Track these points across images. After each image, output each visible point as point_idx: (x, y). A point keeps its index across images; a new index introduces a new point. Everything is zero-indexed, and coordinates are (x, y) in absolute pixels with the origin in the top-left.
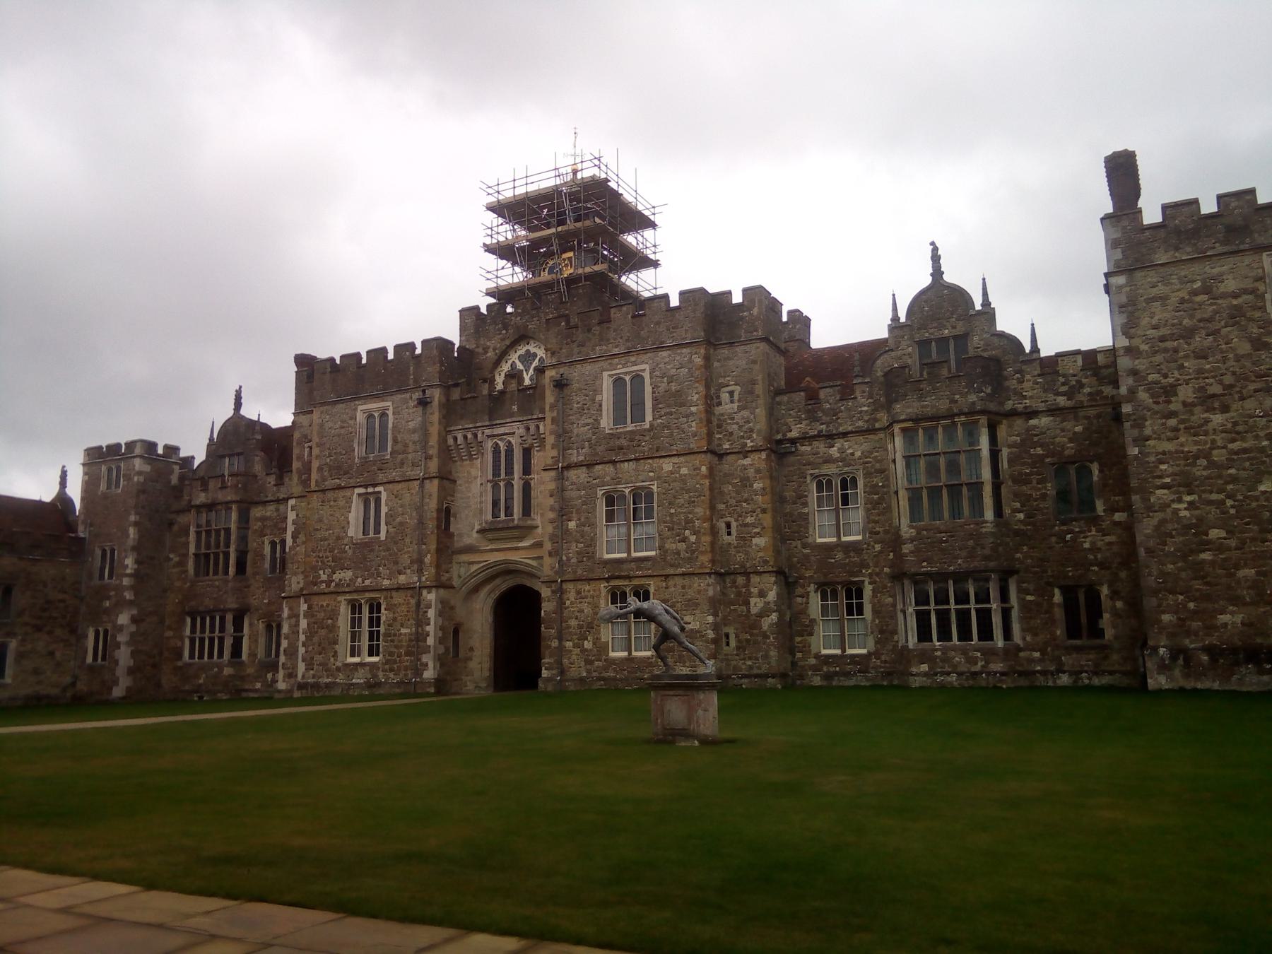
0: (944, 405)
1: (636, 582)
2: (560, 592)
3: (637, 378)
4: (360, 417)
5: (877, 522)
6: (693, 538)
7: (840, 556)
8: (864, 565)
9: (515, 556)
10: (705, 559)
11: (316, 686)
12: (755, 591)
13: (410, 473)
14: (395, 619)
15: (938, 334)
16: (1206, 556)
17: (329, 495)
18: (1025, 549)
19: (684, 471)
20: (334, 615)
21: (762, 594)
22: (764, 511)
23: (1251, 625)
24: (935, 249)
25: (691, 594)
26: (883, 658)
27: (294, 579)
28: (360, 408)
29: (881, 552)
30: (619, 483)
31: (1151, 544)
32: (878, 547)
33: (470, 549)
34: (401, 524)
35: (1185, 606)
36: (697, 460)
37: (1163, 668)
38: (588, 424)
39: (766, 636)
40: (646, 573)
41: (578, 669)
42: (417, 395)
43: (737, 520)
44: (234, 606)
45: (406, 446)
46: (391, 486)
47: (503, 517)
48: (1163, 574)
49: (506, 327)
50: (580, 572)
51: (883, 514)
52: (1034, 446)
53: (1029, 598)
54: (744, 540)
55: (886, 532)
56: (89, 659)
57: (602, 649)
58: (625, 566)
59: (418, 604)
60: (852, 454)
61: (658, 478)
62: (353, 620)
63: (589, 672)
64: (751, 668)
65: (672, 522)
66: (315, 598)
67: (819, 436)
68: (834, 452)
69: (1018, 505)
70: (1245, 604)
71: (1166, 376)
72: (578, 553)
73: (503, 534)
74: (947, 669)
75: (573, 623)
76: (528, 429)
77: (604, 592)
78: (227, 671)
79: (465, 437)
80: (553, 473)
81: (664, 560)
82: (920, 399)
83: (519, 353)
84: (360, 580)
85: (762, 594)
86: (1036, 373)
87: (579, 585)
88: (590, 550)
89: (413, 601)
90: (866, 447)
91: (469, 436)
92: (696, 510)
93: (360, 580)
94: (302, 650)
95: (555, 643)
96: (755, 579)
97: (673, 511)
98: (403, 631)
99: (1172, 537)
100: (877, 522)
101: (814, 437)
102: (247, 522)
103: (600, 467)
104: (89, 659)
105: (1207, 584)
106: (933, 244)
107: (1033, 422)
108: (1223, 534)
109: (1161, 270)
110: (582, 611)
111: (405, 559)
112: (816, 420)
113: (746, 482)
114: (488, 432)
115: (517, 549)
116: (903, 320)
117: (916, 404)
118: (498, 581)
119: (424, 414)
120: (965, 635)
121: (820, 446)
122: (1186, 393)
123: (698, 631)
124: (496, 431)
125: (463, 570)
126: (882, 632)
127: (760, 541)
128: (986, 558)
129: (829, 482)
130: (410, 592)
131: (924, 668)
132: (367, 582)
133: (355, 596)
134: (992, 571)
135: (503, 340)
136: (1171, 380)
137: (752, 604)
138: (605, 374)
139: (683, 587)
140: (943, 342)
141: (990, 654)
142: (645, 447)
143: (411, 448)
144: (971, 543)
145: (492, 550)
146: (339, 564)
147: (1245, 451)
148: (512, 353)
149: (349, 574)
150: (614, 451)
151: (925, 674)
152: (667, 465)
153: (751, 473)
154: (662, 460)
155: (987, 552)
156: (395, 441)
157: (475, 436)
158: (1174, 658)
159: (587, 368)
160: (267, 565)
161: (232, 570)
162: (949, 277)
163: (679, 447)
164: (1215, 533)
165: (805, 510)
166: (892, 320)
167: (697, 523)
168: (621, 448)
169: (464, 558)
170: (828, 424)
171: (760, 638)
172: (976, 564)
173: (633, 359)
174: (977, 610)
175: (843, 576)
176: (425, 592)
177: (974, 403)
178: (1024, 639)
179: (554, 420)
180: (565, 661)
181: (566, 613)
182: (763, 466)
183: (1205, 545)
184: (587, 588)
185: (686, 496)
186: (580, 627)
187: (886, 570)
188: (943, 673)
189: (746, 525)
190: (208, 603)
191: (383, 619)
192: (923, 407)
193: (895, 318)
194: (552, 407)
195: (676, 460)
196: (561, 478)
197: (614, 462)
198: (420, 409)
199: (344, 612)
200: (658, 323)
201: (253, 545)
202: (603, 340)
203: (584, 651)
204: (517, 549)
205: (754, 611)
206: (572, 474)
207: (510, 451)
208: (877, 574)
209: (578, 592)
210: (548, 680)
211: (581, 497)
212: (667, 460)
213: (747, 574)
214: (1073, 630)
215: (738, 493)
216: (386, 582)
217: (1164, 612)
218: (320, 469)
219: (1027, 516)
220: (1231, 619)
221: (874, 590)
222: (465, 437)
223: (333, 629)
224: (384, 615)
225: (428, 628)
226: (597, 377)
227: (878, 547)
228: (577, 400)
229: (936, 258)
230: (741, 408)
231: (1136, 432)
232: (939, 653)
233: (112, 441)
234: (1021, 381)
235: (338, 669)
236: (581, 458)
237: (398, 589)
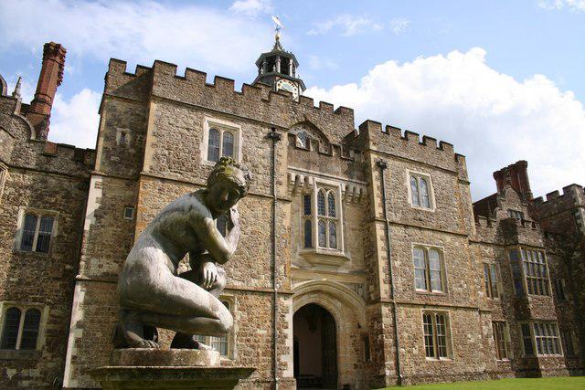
2: (393, 311)
4: (207, 128)
14: (250, 320)
19: (457, 244)
27: (94, 261)
28: (207, 119)
42: (267, 130)
49: (295, 110)
59: (274, 308)
73: (329, 261)
75: (405, 335)
79: (297, 178)
91: (302, 177)
98: (260, 332)
114: (317, 179)
118: (304, 298)
124: (324, 181)
142: (434, 225)
143: (261, 170)
157: (306, 179)
168: (420, 220)
184: (412, 310)
197: (420, 228)
198: (271, 141)
204: (336, 274)
207: (332, 198)
209: (406, 313)
210: (391, 378)
218: (156, 157)
225: (286, 331)
237: (253, 292)
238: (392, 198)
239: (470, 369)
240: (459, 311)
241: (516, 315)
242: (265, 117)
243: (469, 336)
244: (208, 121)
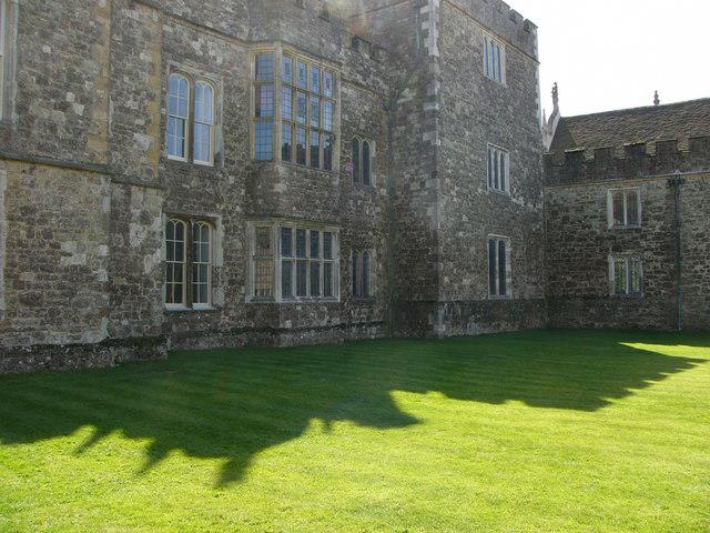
6: (79, 109)
7: (195, 183)
12: (137, 213)
16: (461, 234)
21: (145, 219)
32: (232, 180)
55: (240, 163)
64: (128, 329)
68: (196, 45)
85: (145, 219)
92: (87, 62)
96: (137, 194)
97: (47, 49)
101: (179, 18)
113: (129, 43)
123: (84, 270)
137: (132, 234)
153: (138, 35)
167: (87, 86)
187: (238, 209)
189: (128, 111)
205: (135, 243)
221: (227, 231)
227: (232, 180)
232: (299, 308)
241: (246, 206)
243: (67, 246)
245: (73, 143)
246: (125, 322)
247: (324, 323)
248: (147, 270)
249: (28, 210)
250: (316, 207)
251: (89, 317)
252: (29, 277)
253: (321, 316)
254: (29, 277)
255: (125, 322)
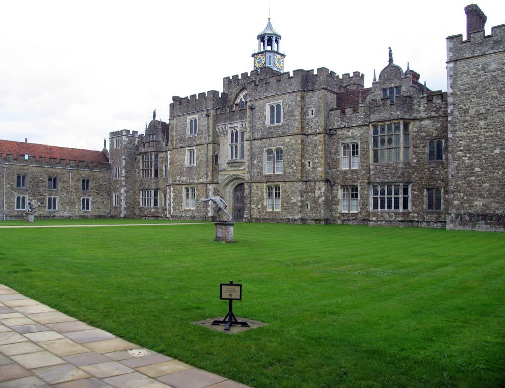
0: (387, 116)
1: (276, 184)
2: (251, 187)
3: (278, 106)
4: (188, 121)
5: (363, 162)
6: (295, 168)
7: (350, 175)
8: (358, 179)
9: (239, 173)
10: (299, 176)
11: (176, 216)
12: (317, 188)
13: (204, 141)
14: (199, 195)
15: (390, 86)
16: (473, 178)
17: (179, 149)
18: (416, 174)
19: (293, 142)
20: (181, 193)
21: (319, 189)
22: (322, 157)
23: (486, 205)
24: (391, 50)
25: (293, 189)
26: (362, 215)
29: (364, 174)
30: (271, 146)
31: (453, 173)
32: (363, 172)
33: (224, 170)
34: (201, 160)
35: (463, 198)
36: (297, 137)
37: (452, 221)
38: (261, 123)
39: (320, 205)
40: (280, 180)
41: (256, 215)
42: (206, 112)
43: (312, 161)
44: (154, 188)
45: (202, 132)
46: (197, 146)
47: (234, 158)
48: (457, 185)
50: (257, 179)
51: (366, 159)
52: (422, 132)
53: (415, 193)
54: (314, 168)
56: (114, 204)
57: (264, 208)
58: (272, 178)
59: (206, 190)
60: (356, 135)
61: (284, 144)
62: (187, 194)
63: (260, 216)
64: (314, 217)
65: (288, 161)
66: (176, 186)
67: (345, 128)
68: (350, 134)
69: (414, 156)
70: (484, 197)
71: (465, 105)
72: (257, 172)
74: (382, 219)
75: (255, 198)
76: (242, 125)
77: (265, 187)
78: (153, 210)
79: (222, 128)
80: (249, 142)
81: (285, 176)
82: (379, 113)
83: (243, 94)
84: (188, 180)
86: (425, 102)
87: (257, 184)
88: (261, 171)
89: (205, 188)
90: (361, 132)
93: (188, 180)
94: (172, 204)
95: (249, 205)
96: (317, 183)
99: (461, 170)
100: (363, 162)
101: (343, 128)
102: (157, 158)
103: (264, 140)
104: (114, 204)
105: (472, 189)
106: (390, 48)
107: (422, 122)
108: (479, 170)
109: (467, 60)
110: (258, 194)
111: (202, 173)
112: (344, 121)
113: (315, 146)
115: (239, 170)
116: (377, 80)
117: (378, 115)
118: (234, 182)
119: (208, 119)
120: (389, 207)
121: (345, 132)
122: (472, 112)
123: (295, 203)
125: (222, 178)
126: (363, 205)
127: (320, 169)
128: (399, 177)
129: (348, 146)
130: (204, 185)
131: (374, 219)
132: (191, 181)
133: (187, 186)
134: (401, 182)
135: (237, 89)
136: (467, 107)
138: (267, 104)
139: (291, 186)
140: (391, 89)
141: (397, 214)
142: (280, 132)
144: (394, 171)
145: (231, 170)
146: (182, 175)
147: (492, 136)
148: (241, 94)
149: (185, 178)
150: (269, 134)
151: (374, 221)
152: (287, 139)
153: (318, 142)
154: (285, 138)
155: (400, 175)
156: (199, 130)
158: (457, 218)
159: (261, 101)
160: (164, 174)
161: (153, 175)
162: (395, 62)
163: (291, 132)
164: (477, 169)
165: (339, 157)
166: (374, 80)
167: (297, 162)
168: (272, 133)
169: (223, 173)
170: (348, 123)
171: (318, 206)
172: (395, 179)
173: (276, 98)
174: (395, 198)
175: (351, 183)
176: (208, 185)
177: (398, 115)
178: (412, 209)
179: (250, 122)
180: (252, 212)
181: (252, 195)
182: (322, 140)
183: (472, 174)
185: (293, 151)
186: (257, 200)
187: (366, 181)
188: (380, 221)
189: (315, 163)
190: (147, 187)
191: (196, 194)
192: (380, 116)
193: (375, 80)
194: (249, 116)
195: (290, 137)
196: (251, 144)
197: (269, 138)
198: (207, 117)
199: (184, 191)
200: (285, 84)
201: (159, 166)
202: (266, 90)
203: (258, 208)
204: (239, 170)
205: (316, 195)
206: (255, 142)
208: (363, 183)
209: (257, 187)
211: (258, 151)
212: (287, 137)
213: (315, 181)
214: (430, 206)
215: (313, 150)
216: (196, 182)
217: (455, 200)
218: (176, 140)
219: (418, 161)
220: (479, 203)
222: (222, 128)
223: (181, 197)
224: (196, 193)
226: (264, 105)
227: (363, 172)
228: (258, 114)
229: (390, 54)
230: (315, 117)
231: (452, 128)
232: (379, 213)
233: (117, 130)
234: (419, 106)
235: (183, 211)
236: (259, 136)
237: (200, 184)
238: (258, 126)
239: (290, 217)
240: (287, 184)
242: (205, 107)
243: (292, 198)
244: (189, 118)
245: (294, 176)
246: (314, 215)
247: (392, 219)
248: (320, 201)
249: (285, 191)
250: (388, 177)
251: (296, 213)
252: (285, 204)
253: (391, 216)
254: (285, 204)
255: (314, 215)
